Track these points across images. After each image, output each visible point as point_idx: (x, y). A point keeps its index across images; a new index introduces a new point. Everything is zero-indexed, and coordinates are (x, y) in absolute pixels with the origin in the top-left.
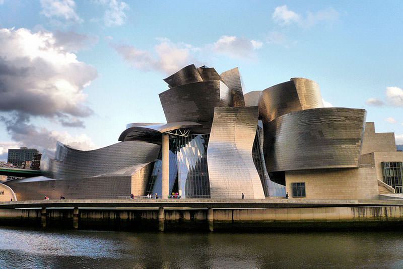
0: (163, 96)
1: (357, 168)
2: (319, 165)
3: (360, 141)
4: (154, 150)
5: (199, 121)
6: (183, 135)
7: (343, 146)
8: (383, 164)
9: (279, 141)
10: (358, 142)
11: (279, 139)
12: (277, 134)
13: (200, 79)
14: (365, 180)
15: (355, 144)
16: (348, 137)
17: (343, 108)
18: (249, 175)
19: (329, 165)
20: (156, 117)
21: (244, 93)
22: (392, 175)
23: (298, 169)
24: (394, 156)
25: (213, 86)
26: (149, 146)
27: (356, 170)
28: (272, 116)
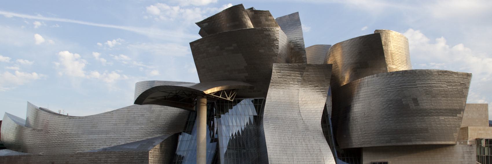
0: (194, 45)
1: (453, 145)
2: (410, 141)
3: (462, 112)
4: (179, 117)
5: (247, 81)
6: (229, 99)
7: (442, 118)
8: (478, 141)
9: (355, 110)
10: (460, 114)
11: (355, 108)
12: (354, 100)
13: (250, 25)
14: (462, 160)
15: (456, 116)
16: (448, 107)
17: (446, 72)
18: (321, 151)
19: (422, 141)
20: (185, 73)
21: (306, 47)
22: (486, 154)
23: (383, 145)
24: (489, 132)
25: (269, 35)
26: (171, 112)
27: (451, 148)
28: (346, 78)
